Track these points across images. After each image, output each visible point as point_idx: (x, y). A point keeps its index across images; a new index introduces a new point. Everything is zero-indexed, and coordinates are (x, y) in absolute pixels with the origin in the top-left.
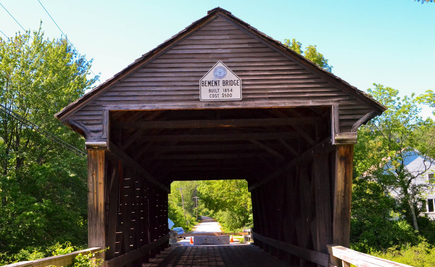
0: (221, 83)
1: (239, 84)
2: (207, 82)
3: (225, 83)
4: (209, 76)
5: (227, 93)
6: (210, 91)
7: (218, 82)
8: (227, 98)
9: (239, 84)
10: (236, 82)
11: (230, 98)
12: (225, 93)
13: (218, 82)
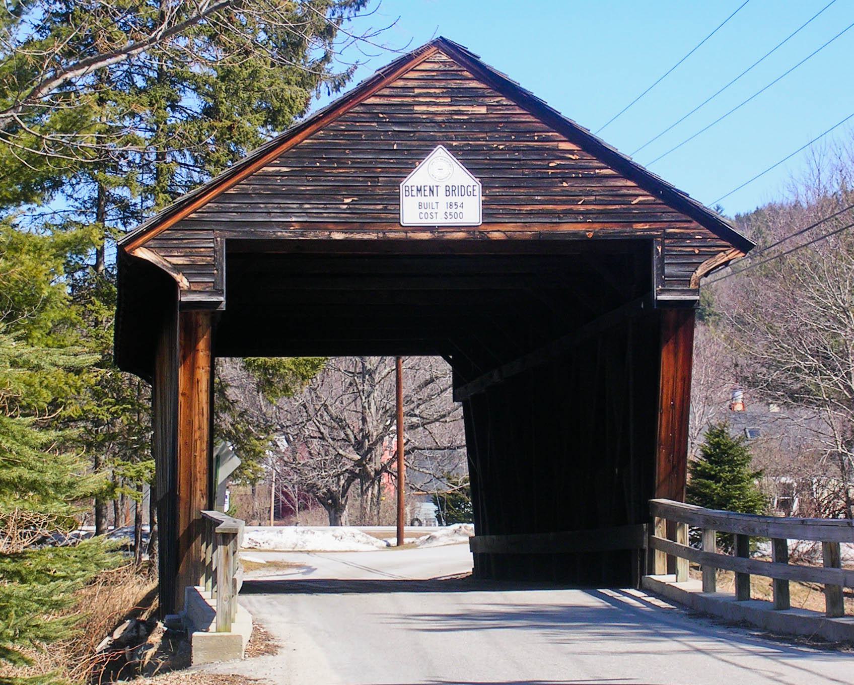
0: (442, 191)
1: (476, 193)
2: (415, 189)
3: (451, 191)
4: (418, 177)
5: (453, 210)
6: (420, 205)
7: (435, 188)
8: (453, 220)
9: (476, 193)
10: (470, 189)
11: (458, 220)
12: (449, 211)
13: (435, 188)
